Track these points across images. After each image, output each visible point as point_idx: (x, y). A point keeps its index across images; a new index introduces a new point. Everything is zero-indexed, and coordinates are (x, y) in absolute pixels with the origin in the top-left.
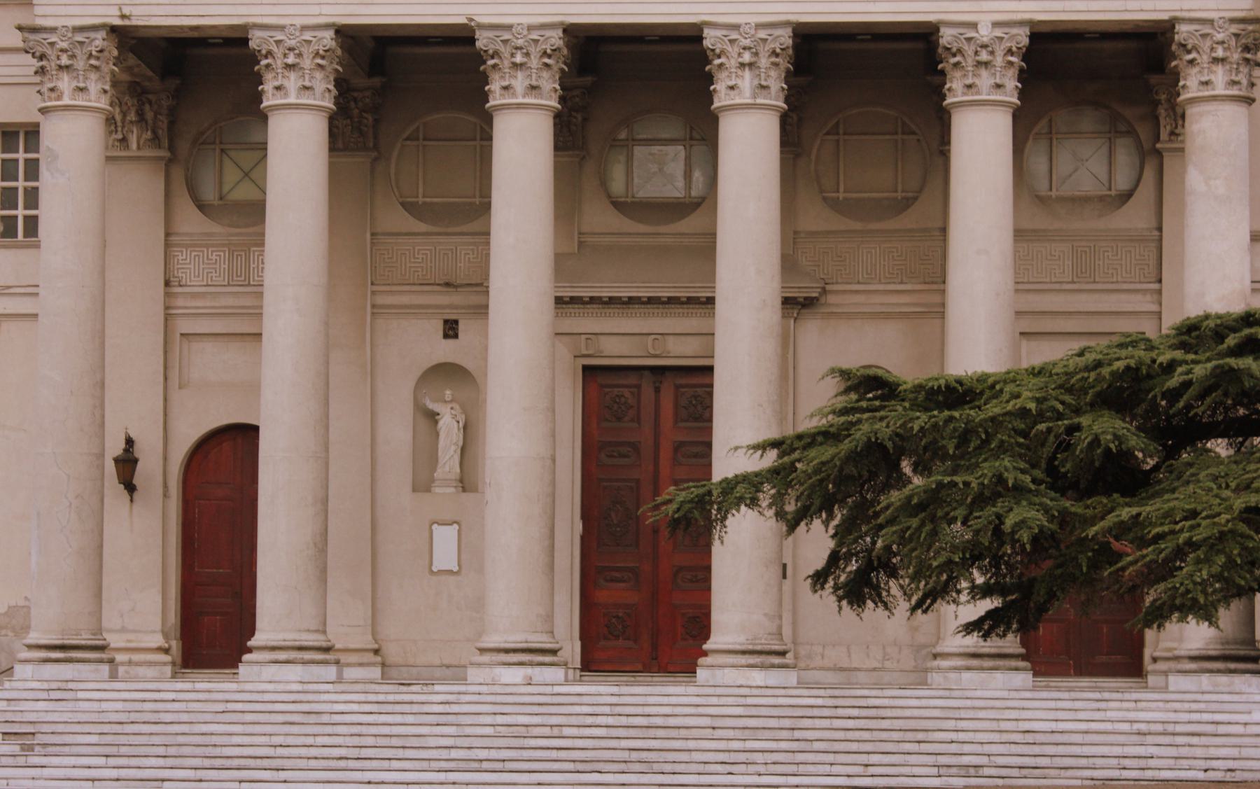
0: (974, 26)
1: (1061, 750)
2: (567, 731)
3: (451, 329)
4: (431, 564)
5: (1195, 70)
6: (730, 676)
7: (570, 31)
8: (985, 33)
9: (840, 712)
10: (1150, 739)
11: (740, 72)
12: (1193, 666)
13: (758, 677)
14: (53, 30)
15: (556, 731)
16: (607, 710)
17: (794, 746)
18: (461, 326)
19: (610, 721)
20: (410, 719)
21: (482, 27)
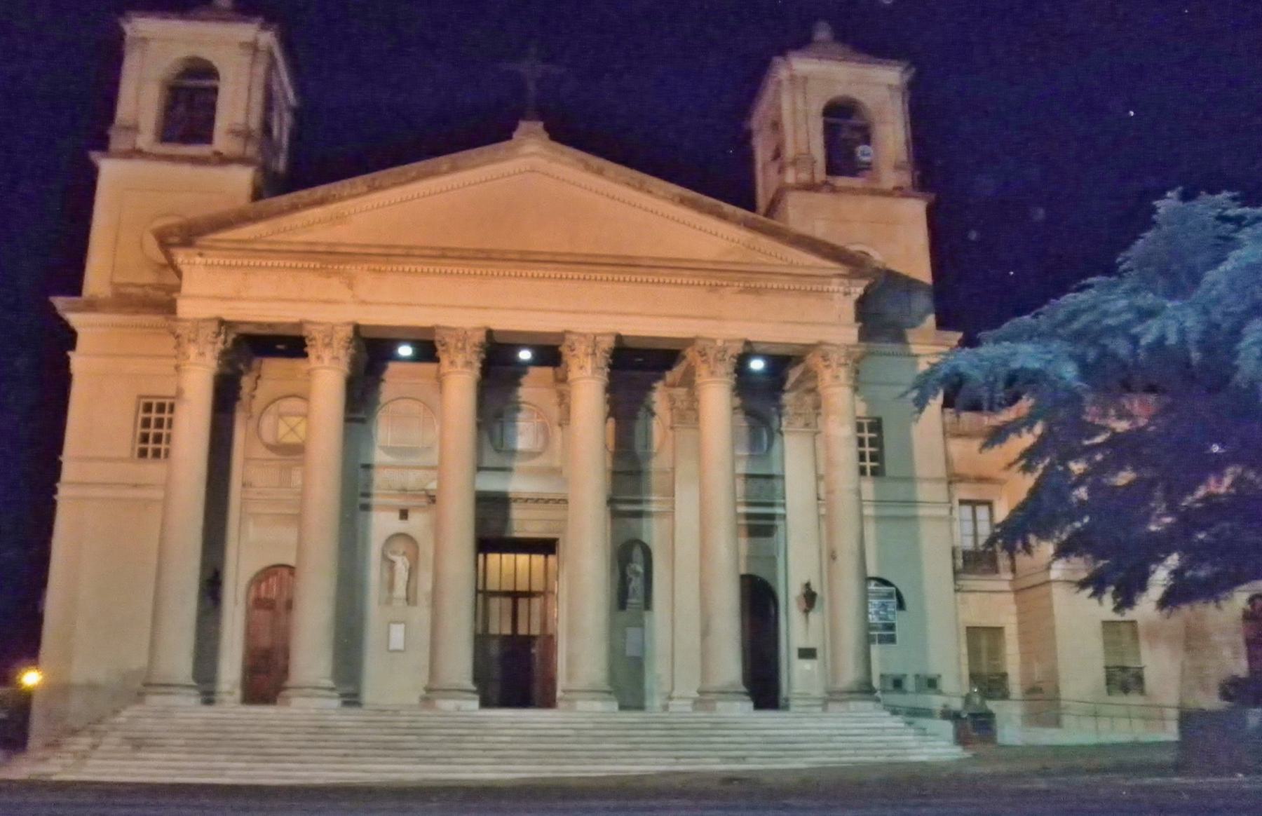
0: (714, 340)
1: (787, 746)
2: (486, 738)
3: (404, 514)
4: (388, 646)
5: (830, 370)
6: (582, 705)
7: (490, 333)
8: (719, 343)
9: (650, 726)
10: (834, 739)
11: (585, 360)
12: (847, 696)
13: (598, 706)
14: (186, 320)
15: (479, 738)
16: (509, 725)
17: (628, 746)
18: (410, 514)
19: (512, 732)
20: (386, 731)
21: (438, 327)
